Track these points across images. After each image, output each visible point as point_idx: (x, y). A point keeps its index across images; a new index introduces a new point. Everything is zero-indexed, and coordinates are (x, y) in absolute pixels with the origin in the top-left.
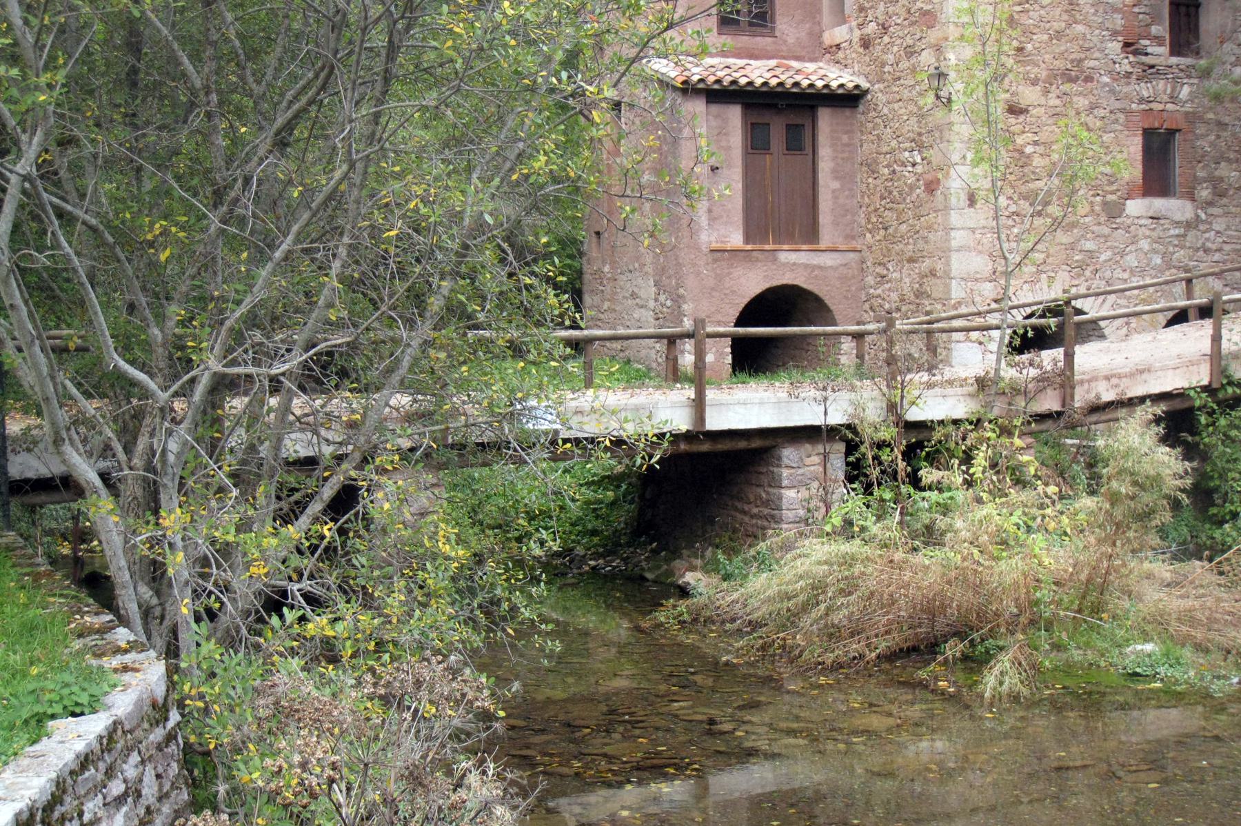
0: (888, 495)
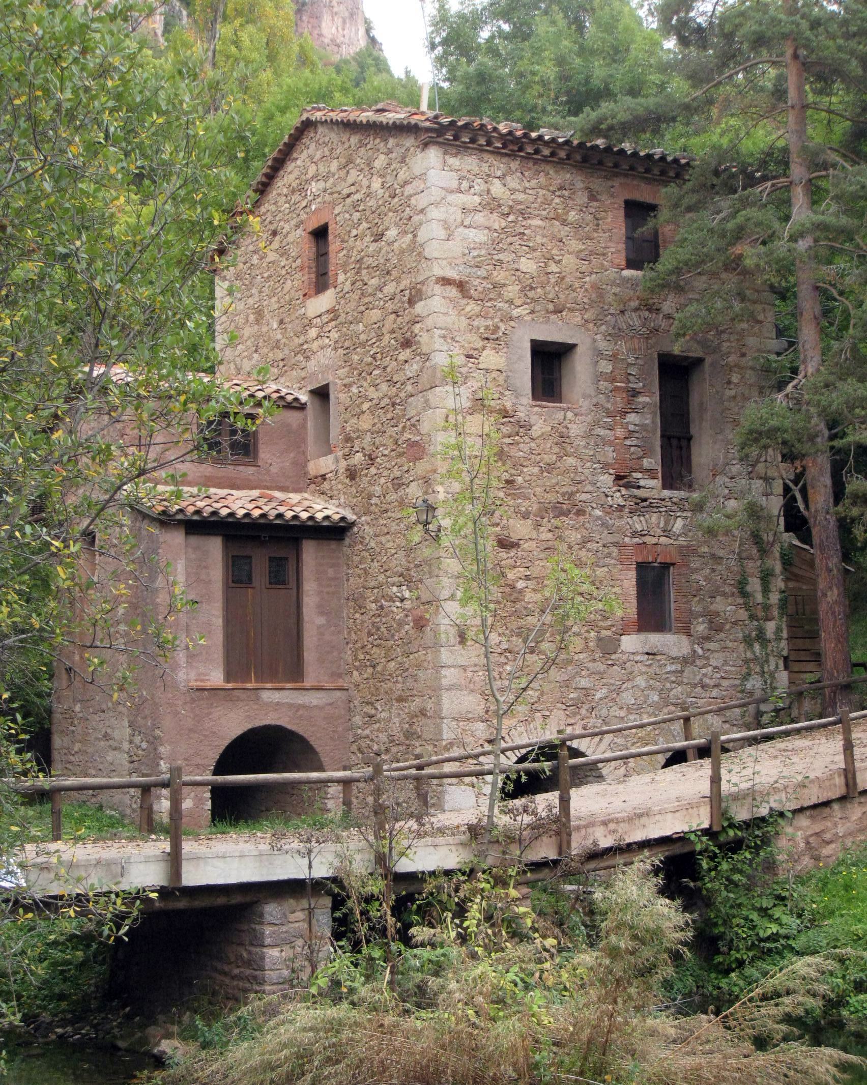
0: (377, 953)
